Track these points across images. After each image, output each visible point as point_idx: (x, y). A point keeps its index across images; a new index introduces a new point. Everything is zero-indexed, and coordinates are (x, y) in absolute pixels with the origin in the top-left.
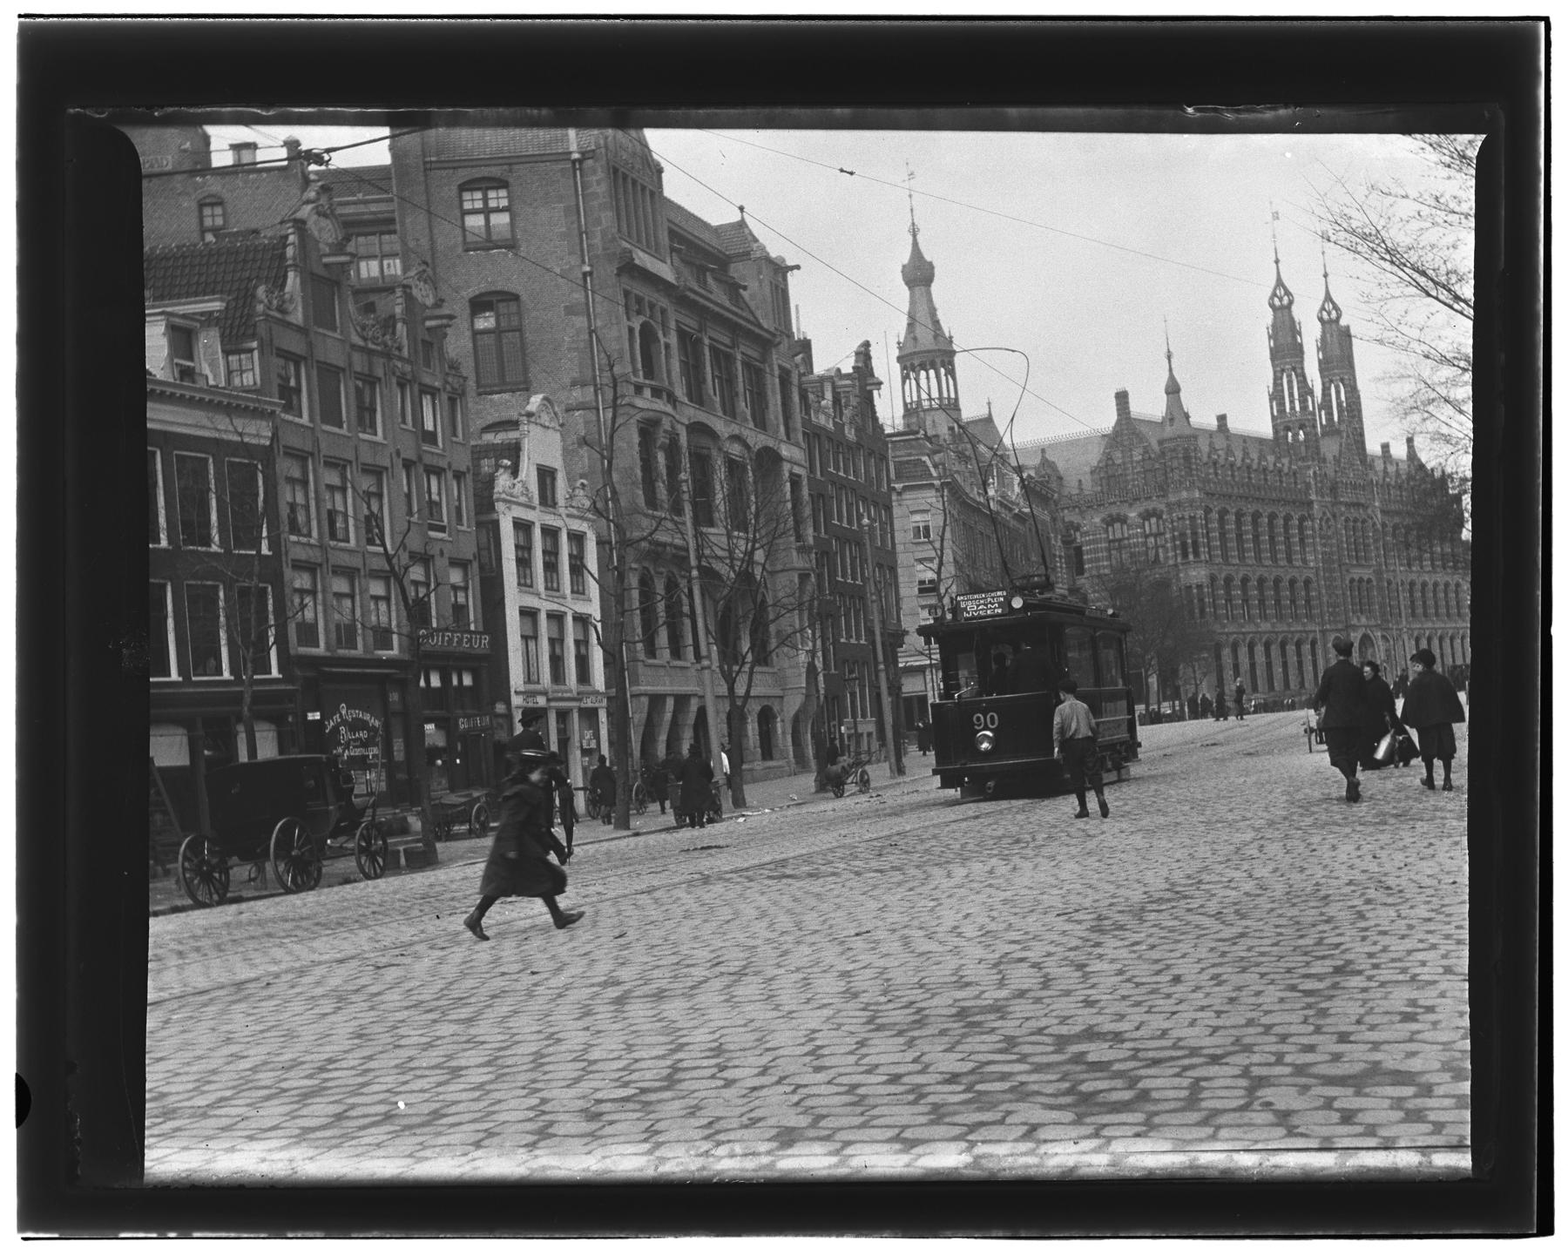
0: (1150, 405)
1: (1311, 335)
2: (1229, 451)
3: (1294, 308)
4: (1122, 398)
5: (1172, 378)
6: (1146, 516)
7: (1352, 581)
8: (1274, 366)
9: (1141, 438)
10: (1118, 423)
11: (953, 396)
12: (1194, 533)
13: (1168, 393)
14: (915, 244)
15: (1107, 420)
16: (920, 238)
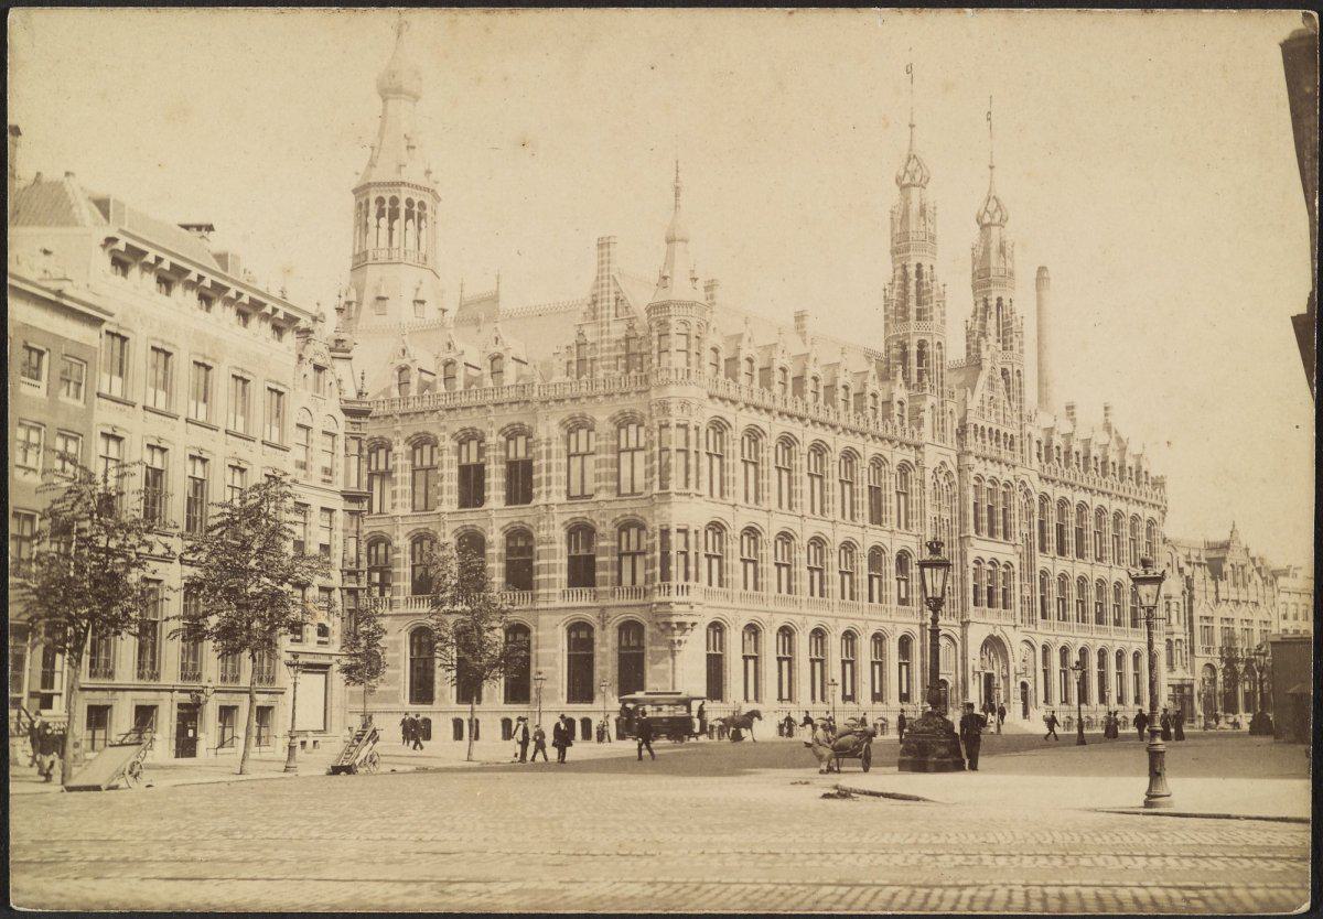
3: (929, 186)
4: (603, 244)
7: (978, 561)
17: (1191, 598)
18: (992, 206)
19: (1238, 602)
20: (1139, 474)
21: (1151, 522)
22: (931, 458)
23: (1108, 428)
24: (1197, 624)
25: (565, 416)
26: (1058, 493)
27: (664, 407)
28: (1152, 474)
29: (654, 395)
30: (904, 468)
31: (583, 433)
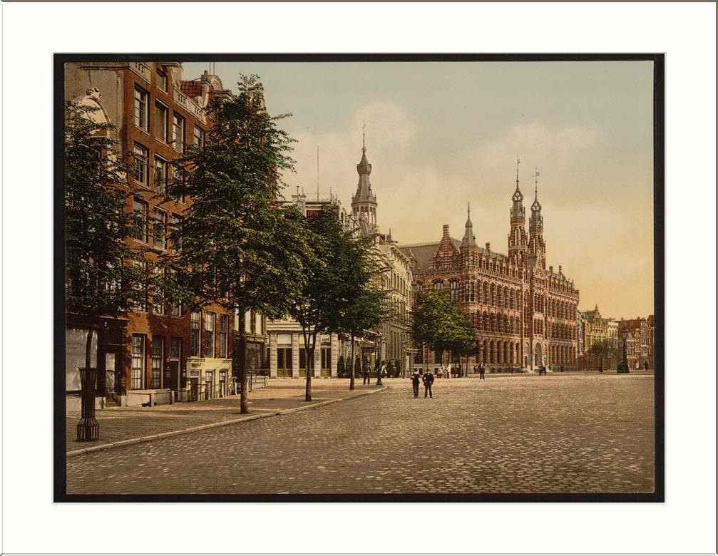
0: (457, 234)
1: (528, 214)
2: (488, 257)
3: (523, 202)
4: (446, 227)
5: (469, 220)
6: (451, 281)
8: (512, 225)
9: (451, 244)
10: (443, 239)
11: (374, 223)
12: (473, 291)
13: (466, 227)
14: (364, 155)
15: (437, 238)
16: (366, 153)
17: (584, 330)
18: (536, 204)
19: (597, 331)
20: (572, 289)
21: (575, 305)
22: (524, 290)
23: (560, 273)
24: (586, 338)
25: (434, 279)
26: (485, 279)
27: (467, 277)
28: (575, 289)
29: (463, 274)
30: (518, 291)
31: (439, 284)
